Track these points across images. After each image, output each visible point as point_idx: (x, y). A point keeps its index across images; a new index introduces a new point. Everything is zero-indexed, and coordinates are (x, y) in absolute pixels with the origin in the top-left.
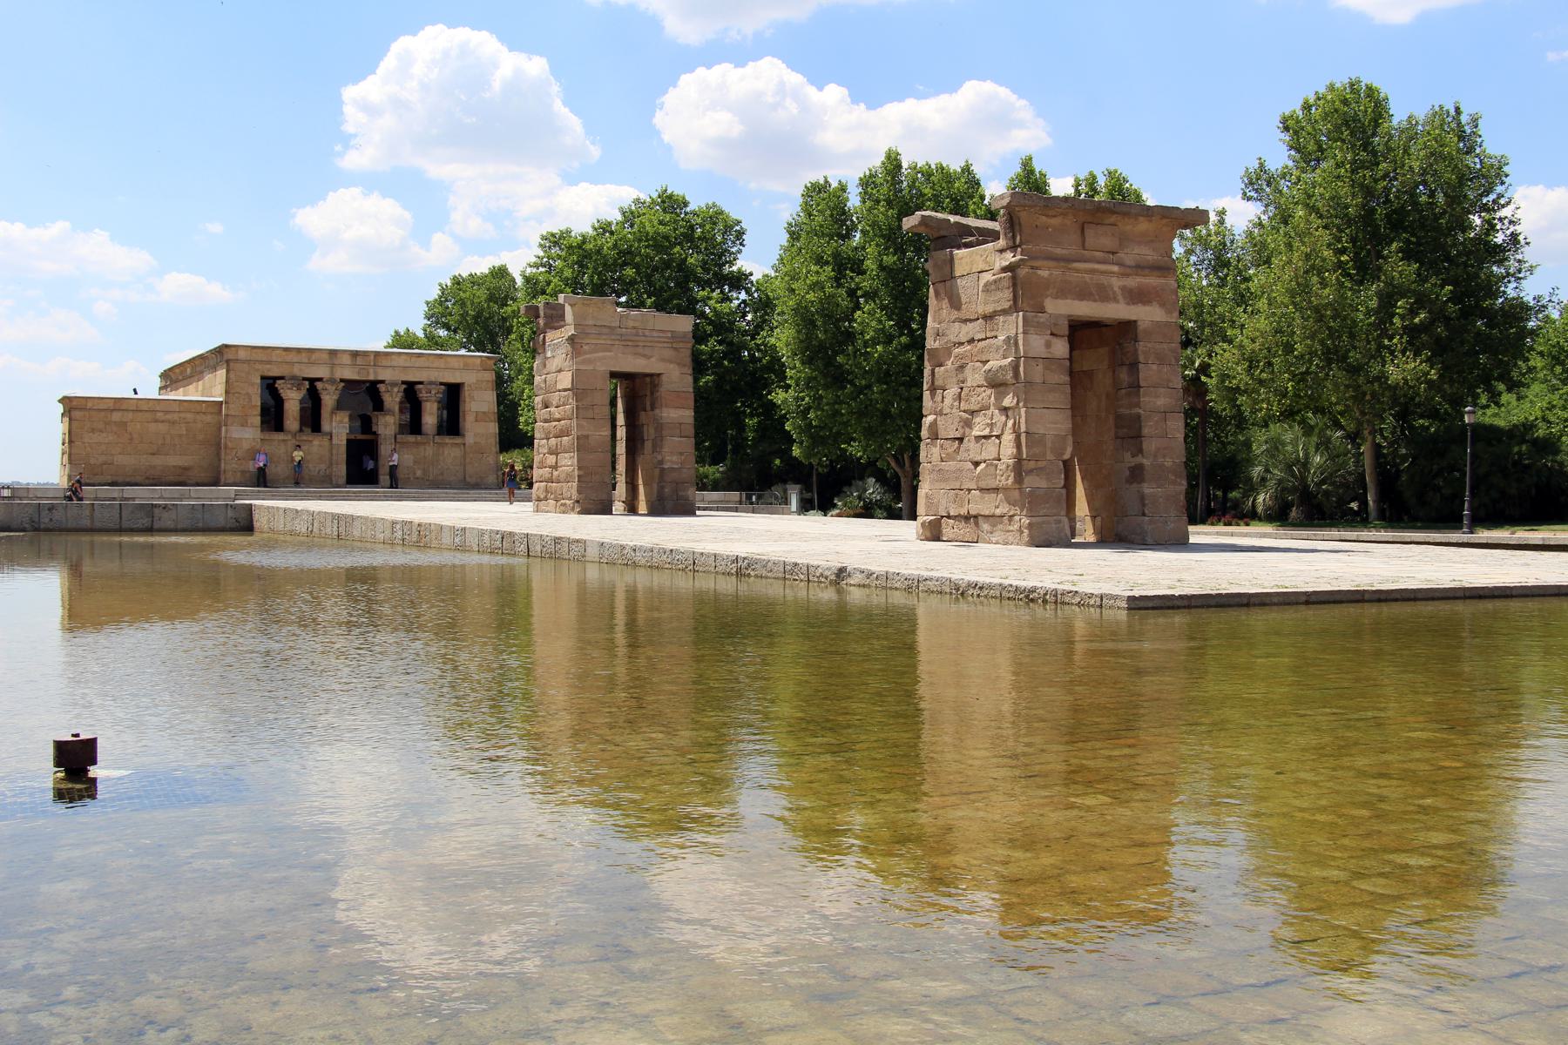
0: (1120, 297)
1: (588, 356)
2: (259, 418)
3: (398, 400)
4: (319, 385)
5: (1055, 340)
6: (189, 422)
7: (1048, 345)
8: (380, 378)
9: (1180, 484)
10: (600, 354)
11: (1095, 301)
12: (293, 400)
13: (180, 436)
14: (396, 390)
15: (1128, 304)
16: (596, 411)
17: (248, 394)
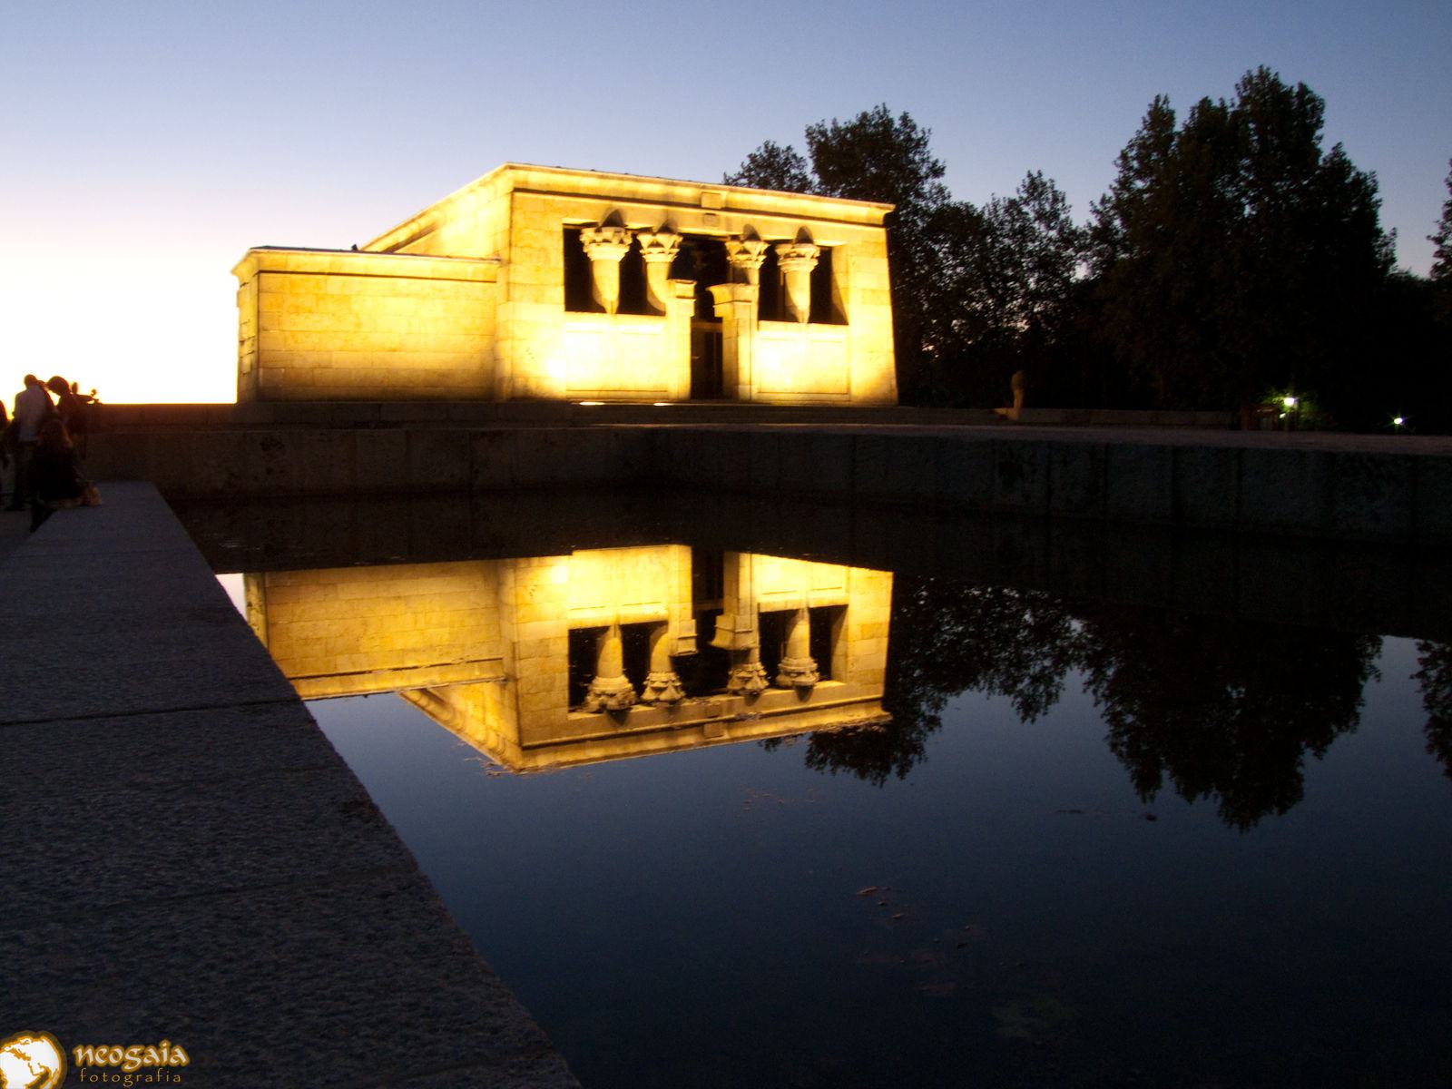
3: (758, 265)
4: (645, 239)
8: (738, 231)
12: (606, 258)
17: (543, 249)
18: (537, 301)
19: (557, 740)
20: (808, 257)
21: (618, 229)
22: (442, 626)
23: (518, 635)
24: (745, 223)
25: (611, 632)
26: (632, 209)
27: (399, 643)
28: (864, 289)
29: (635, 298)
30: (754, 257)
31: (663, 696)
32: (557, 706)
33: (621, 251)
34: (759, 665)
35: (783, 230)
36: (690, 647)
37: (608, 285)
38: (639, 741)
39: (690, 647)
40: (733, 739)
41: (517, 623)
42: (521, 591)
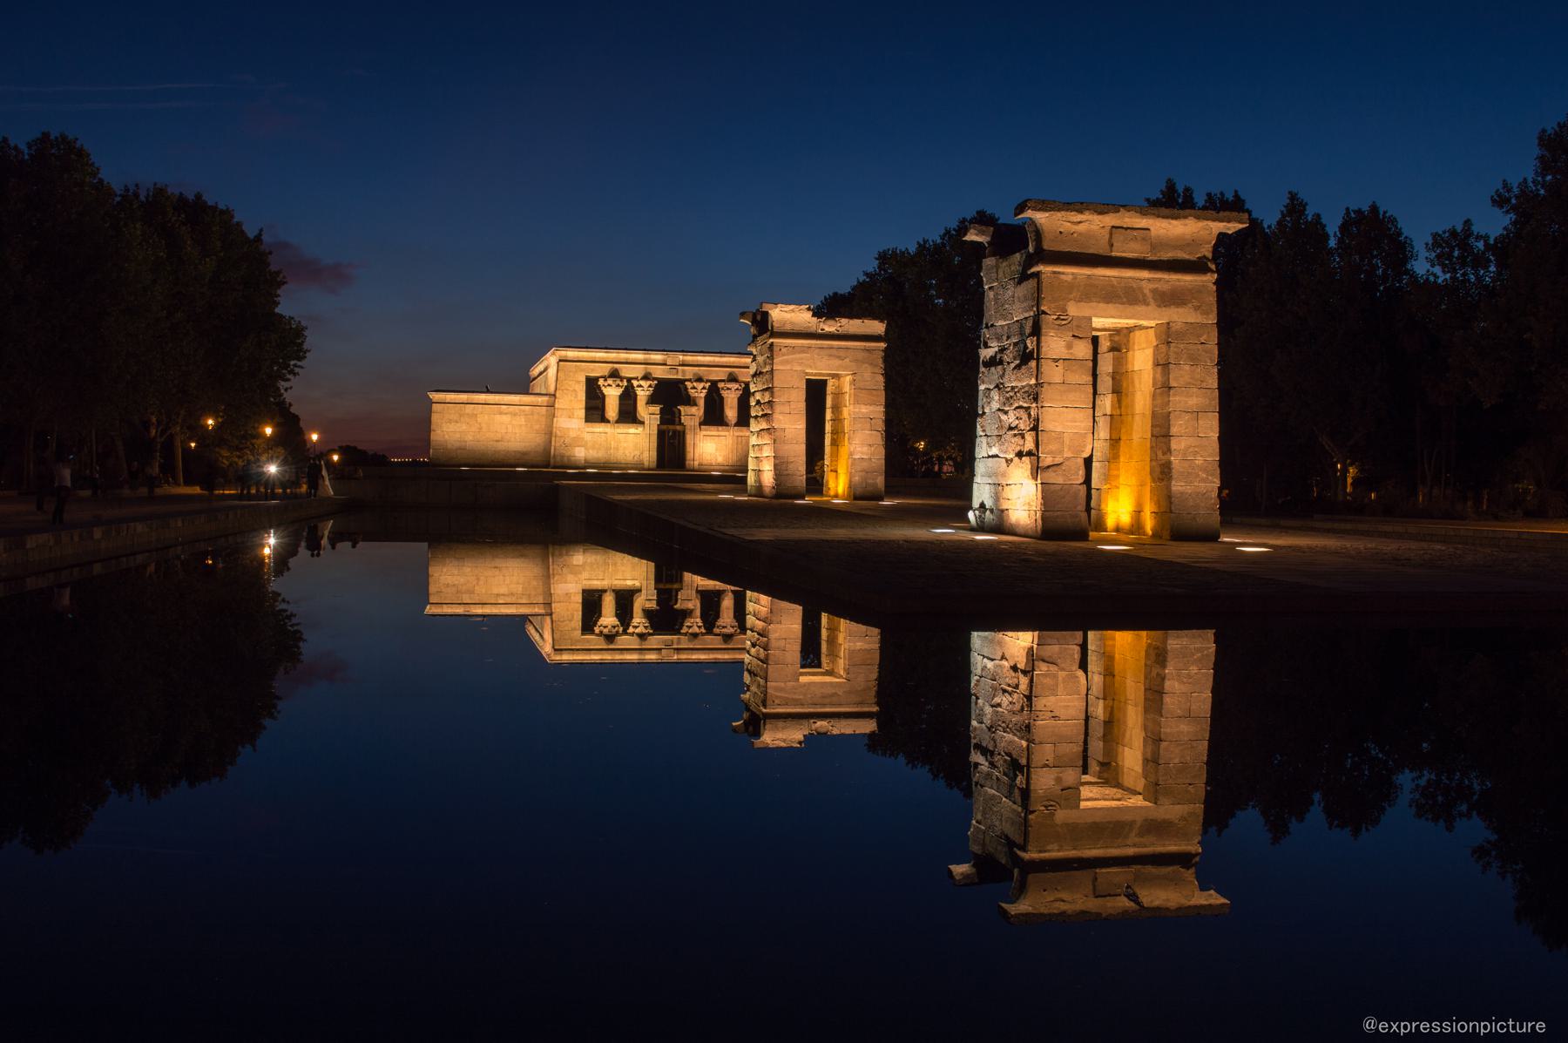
0: (1152, 301)
1: (785, 357)
2: (584, 411)
3: (703, 395)
4: (635, 383)
5: (1077, 342)
6: (526, 415)
7: (1069, 346)
10: (798, 356)
11: (1123, 303)
12: (612, 393)
13: (521, 426)
14: (700, 386)
15: (1159, 306)
16: (792, 407)
17: (575, 390)
18: (570, 417)
20: (733, 390)
26: (626, 368)
27: (495, 591)
29: (628, 414)
30: (699, 391)
31: (637, 631)
32: (575, 629)
33: (619, 391)
34: (699, 620)
36: (653, 605)
37: (612, 409)
38: (622, 654)
39: (653, 605)
40: (678, 659)
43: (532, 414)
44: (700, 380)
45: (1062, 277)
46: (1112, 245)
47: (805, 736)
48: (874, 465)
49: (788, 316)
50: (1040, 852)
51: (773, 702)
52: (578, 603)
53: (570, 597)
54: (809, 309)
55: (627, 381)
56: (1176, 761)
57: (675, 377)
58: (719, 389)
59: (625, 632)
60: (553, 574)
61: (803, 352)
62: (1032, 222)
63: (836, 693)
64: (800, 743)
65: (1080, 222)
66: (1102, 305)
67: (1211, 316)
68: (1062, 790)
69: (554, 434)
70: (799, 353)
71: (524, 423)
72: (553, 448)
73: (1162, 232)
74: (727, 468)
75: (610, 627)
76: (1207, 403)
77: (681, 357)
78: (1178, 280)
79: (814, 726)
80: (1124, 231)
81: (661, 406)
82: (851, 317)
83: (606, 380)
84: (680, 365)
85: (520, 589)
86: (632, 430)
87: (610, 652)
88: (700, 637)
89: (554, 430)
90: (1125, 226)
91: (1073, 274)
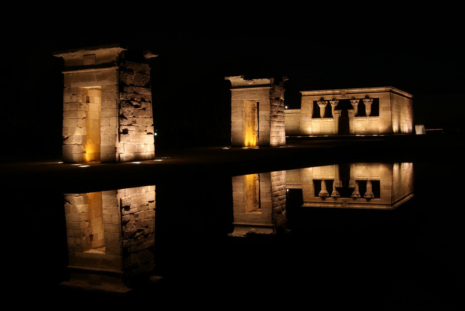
0: (96, 79)
1: (235, 96)
4: (331, 102)
7: (71, 98)
9: (114, 142)
10: (239, 95)
12: (322, 107)
13: (292, 121)
14: (354, 101)
15: (98, 81)
17: (308, 107)
18: (306, 117)
19: (311, 201)
21: (321, 101)
22: (293, 177)
23: (302, 180)
24: (352, 96)
25: (322, 181)
26: (326, 97)
28: (383, 107)
29: (328, 115)
31: (333, 196)
32: (310, 194)
35: (362, 96)
37: (322, 112)
41: (302, 177)
42: (303, 171)
43: (296, 116)
44: (354, 99)
45: (70, 75)
46: (83, 61)
47: (247, 233)
48: (266, 133)
49: (236, 80)
50: (72, 266)
51: (236, 220)
52: (311, 185)
53: (308, 182)
54: (241, 77)
55: (328, 102)
56: (110, 239)
57: (344, 99)
58: (363, 102)
59: (330, 196)
60: (302, 174)
61: (241, 93)
62: (61, 57)
63: (257, 218)
64: (244, 236)
65: (74, 55)
66: (81, 83)
67: (115, 82)
68: (77, 245)
69: (301, 123)
70: (240, 94)
71: (293, 120)
72: (300, 128)
73: (99, 54)
74: (366, 133)
75: (322, 194)
76: (113, 113)
77: (346, 91)
78: (105, 71)
79: (250, 230)
80: (87, 56)
81: (340, 111)
82: (257, 78)
83: (319, 102)
84: (346, 94)
85: (294, 179)
86: (329, 120)
87: (323, 203)
88: (358, 199)
89: (301, 122)
90: (87, 54)
91: (73, 73)
